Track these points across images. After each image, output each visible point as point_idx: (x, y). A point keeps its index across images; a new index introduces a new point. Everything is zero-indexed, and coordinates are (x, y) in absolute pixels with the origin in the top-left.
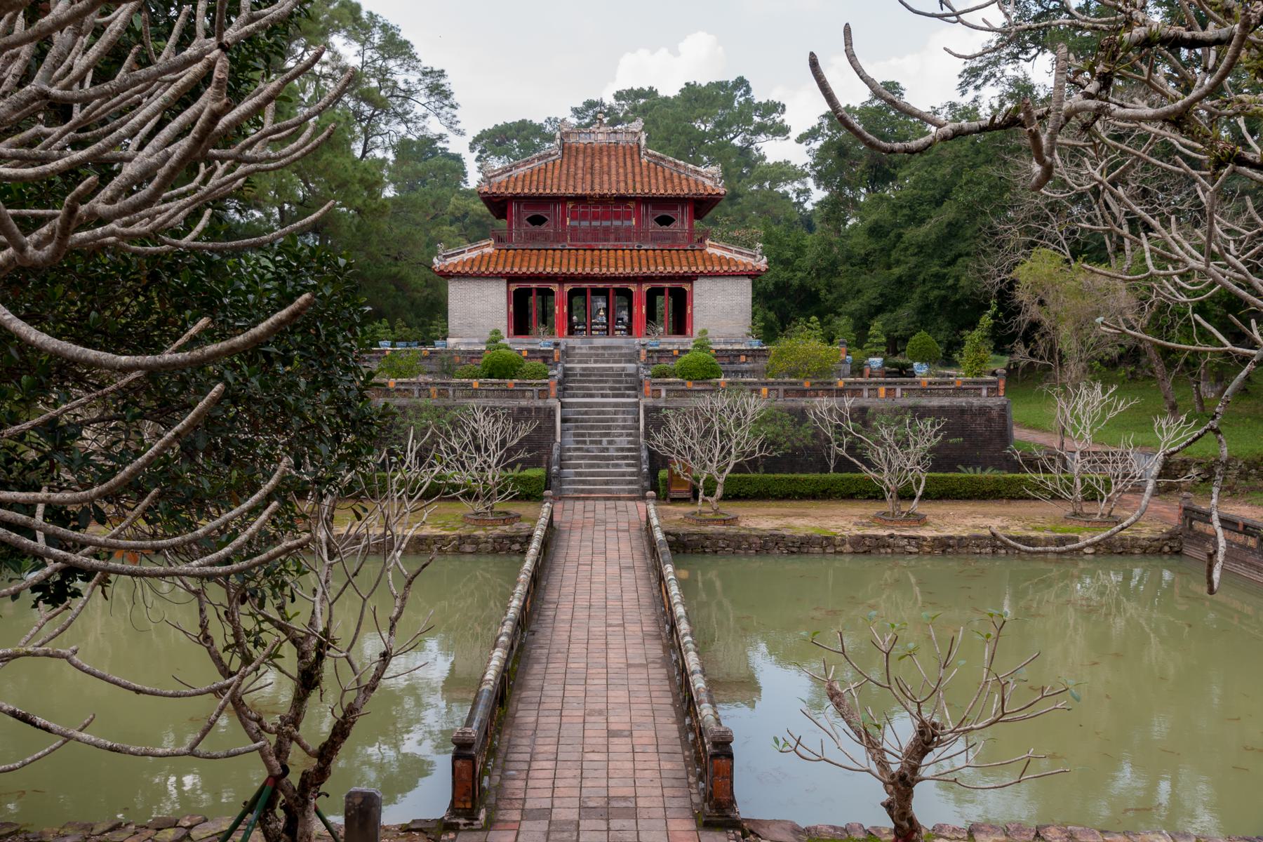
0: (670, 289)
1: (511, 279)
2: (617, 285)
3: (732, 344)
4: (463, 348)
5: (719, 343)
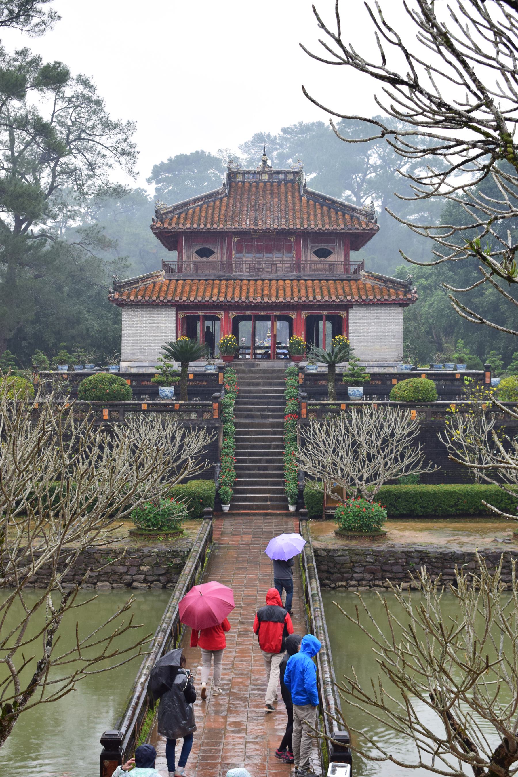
0: (327, 316)
1: (179, 307)
2: (278, 313)
3: (385, 367)
4: (134, 371)
5: (372, 367)
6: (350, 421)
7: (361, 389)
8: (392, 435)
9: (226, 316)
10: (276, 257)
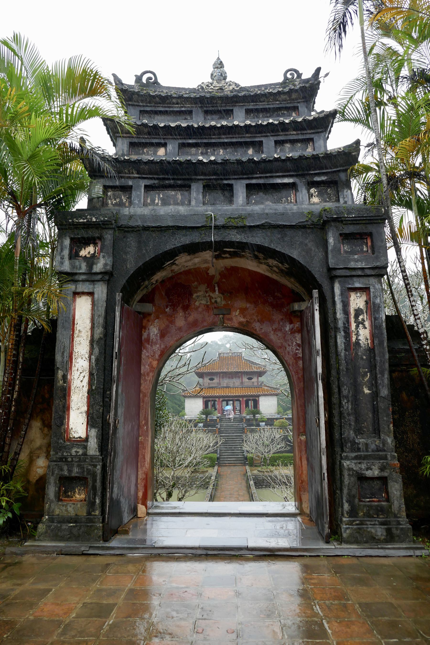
1: (204, 397)
6: (261, 433)
7: (264, 423)
8: (275, 438)
9: (219, 399)
10: (234, 380)
